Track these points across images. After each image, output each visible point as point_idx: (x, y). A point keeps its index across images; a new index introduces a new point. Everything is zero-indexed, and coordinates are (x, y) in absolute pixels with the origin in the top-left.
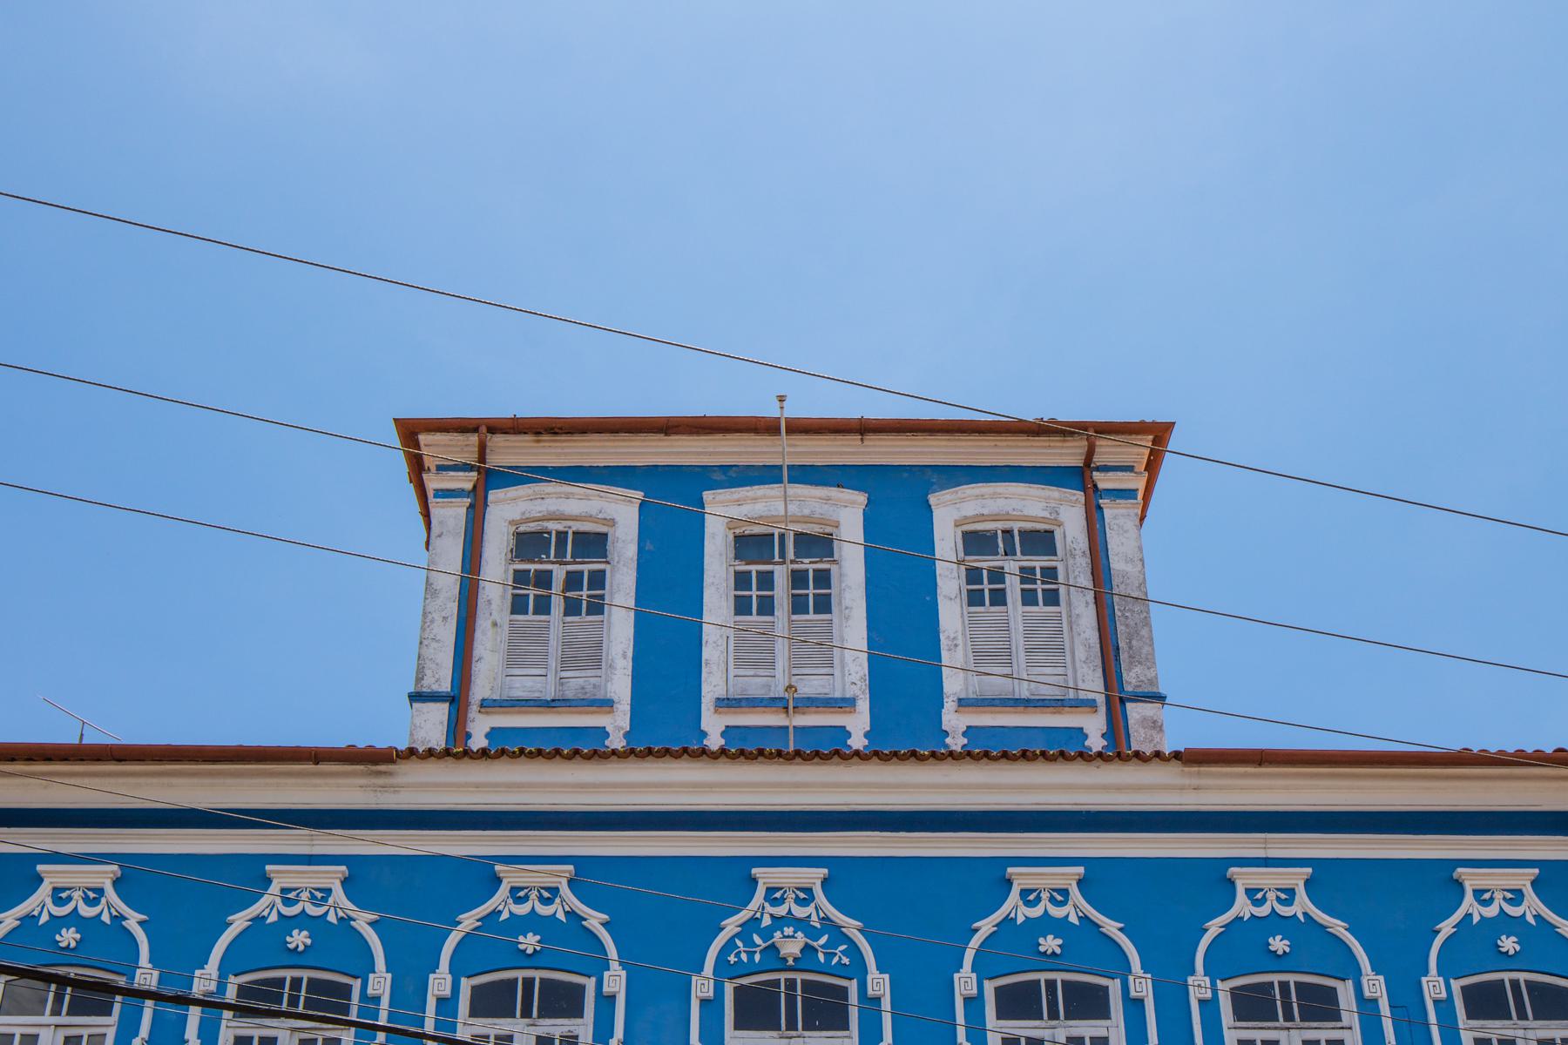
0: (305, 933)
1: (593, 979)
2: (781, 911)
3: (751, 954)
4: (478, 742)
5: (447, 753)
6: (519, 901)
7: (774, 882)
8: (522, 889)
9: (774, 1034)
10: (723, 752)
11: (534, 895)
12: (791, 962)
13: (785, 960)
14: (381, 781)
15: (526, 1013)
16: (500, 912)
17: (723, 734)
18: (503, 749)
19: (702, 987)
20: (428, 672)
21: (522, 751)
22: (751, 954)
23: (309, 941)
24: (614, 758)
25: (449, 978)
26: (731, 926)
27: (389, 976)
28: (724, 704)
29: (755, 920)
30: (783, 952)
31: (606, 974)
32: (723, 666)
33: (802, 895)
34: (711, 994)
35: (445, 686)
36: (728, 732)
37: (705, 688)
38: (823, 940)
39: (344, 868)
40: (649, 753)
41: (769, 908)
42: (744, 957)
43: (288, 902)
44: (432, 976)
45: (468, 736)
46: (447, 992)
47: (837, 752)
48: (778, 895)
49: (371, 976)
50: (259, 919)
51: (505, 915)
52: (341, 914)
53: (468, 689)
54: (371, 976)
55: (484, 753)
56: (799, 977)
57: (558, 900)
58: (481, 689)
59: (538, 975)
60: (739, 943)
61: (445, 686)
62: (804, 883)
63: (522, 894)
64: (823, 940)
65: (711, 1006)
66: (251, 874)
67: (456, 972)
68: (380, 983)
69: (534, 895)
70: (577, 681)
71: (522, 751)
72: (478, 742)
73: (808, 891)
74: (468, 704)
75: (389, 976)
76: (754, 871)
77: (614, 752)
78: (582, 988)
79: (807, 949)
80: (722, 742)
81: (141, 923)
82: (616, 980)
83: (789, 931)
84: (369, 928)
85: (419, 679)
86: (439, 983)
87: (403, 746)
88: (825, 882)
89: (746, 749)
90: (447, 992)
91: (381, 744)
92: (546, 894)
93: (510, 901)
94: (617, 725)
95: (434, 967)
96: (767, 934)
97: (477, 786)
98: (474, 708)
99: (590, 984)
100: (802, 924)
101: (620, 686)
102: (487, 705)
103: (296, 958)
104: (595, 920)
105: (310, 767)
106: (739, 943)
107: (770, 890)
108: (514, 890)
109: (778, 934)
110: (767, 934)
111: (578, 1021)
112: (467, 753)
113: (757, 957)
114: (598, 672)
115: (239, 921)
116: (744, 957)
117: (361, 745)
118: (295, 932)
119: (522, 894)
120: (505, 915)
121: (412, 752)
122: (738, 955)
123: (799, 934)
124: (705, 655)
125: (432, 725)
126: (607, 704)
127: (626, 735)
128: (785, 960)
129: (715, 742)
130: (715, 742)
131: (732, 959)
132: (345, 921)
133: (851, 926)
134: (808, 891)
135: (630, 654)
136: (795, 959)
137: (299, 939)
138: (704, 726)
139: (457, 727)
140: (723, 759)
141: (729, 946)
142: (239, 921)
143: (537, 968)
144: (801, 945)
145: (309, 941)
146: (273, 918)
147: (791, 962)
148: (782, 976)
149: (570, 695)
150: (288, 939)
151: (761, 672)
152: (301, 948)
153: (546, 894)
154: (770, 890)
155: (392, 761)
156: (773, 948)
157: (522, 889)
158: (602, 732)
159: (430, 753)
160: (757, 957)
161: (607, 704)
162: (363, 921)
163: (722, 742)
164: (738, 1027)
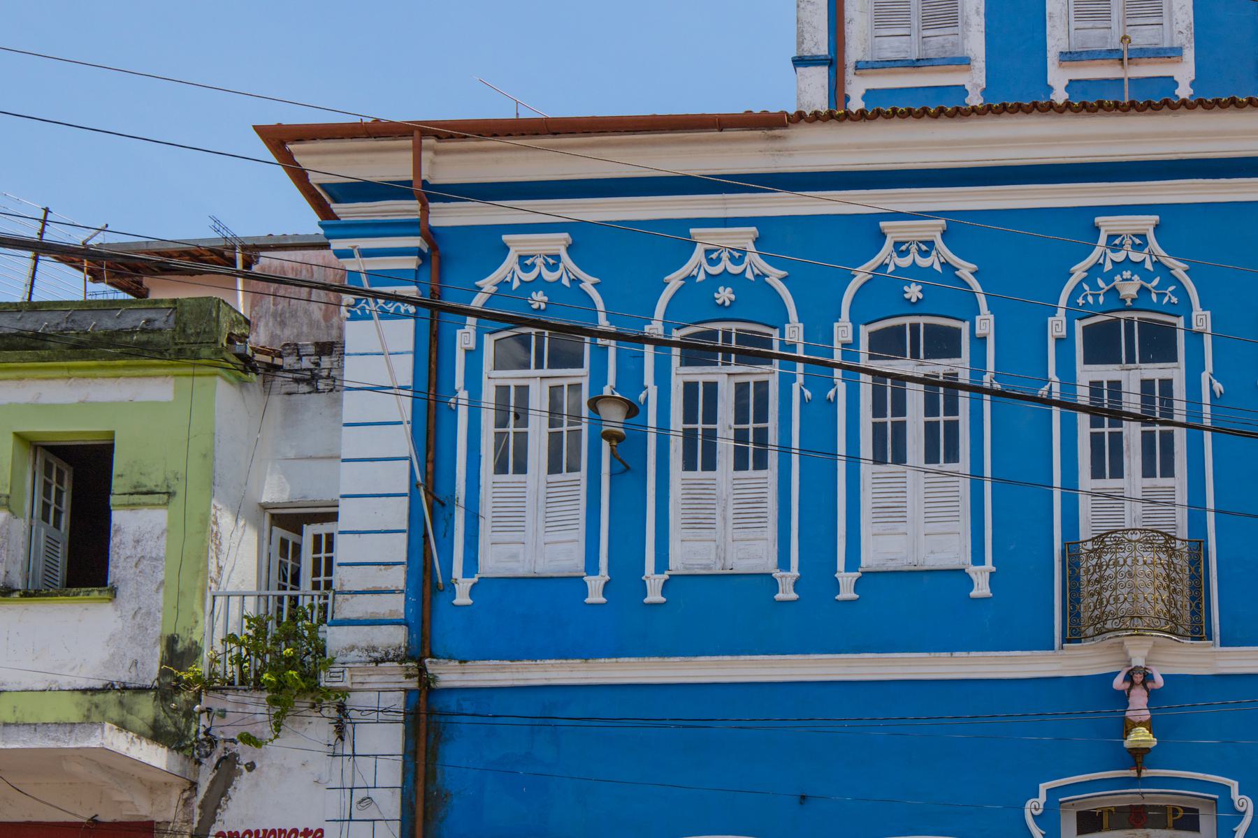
0: (729, 289)
1: (967, 323)
2: (1120, 257)
3: (1096, 296)
4: (856, 105)
5: (830, 116)
6: (902, 254)
7: (1115, 230)
8: (904, 243)
9: (1116, 366)
10: (1068, 106)
11: (914, 248)
12: (1129, 303)
13: (1124, 300)
14: (777, 145)
15: (915, 355)
16: (887, 265)
17: (1067, 88)
18: (880, 110)
19: (1057, 325)
20: (807, 36)
21: (894, 110)
22: (1096, 296)
23: (733, 297)
24: (974, 115)
25: (850, 325)
26: (1079, 271)
27: (801, 325)
28: (1069, 57)
29: (1098, 265)
30: (1123, 293)
31: (978, 318)
32: (1065, 18)
33: (1138, 241)
34: (1064, 333)
35: (823, 50)
36: (1072, 85)
37: (1050, 42)
38: (1156, 282)
39: (754, 229)
40: (1003, 109)
41: (1110, 255)
42: (1090, 299)
43: (712, 262)
44: (836, 325)
45: (847, 98)
46: (849, 339)
47: (1166, 103)
48: (1117, 242)
49: (787, 326)
50: (690, 278)
51: (891, 268)
52: (756, 271)
53: (843, 52)
54: (787, 326)
55: (862, 115)
56: (1136, 316)
57: (934, 253)
58: (854, 52)
59: (922, 321)
60: (1086, 287)
61: (823, 50)
62: (1139, 229)
63: (904, 248)
64: (1156, 282)
65: (1064, 344)
66: (675, 240)
67: (856, 320)
68: (795, 332)
69: (914, 248)
70: (939, 40)
71: (894, 110)
72: (856, 105)
73: (1143, 237)
74: (844, 67)
75: (801, 325)
76: (1097, 220)
77: (974, 109)
78: (959, 331)
79: (1143, 290)
80: (1066, 96)
81: (594, 285)
82: (986, 324)
83: (1127, 274)
84: (780, 283)
85: (800, 43)
86: (842, 331)
87: (792, 111)
88: (1157, 228)
89: (1089, 102)
90: (849, 339)
91: (774, 109)
92: (924, 248)
93: (894, 254)
94: (974, 82)
95: (837, 316)
96: (1109, 278)
97: (859, 147)
98: (850, 70)
99: (965, 327)
100: (1137, 266)
101: (975, 45)
102: (860, 67)
103: (724, 313)
104: (966, 270)
105: (715, 134)
106: (1086, 287)
107: (1111, 237)
108: (897, 244)
109: (1118, 278)
110: (1109, 278)
111: (957, 360)
112: (848, 116)
113: (1101, 299)
114: (955, 30)
115: (674, 281)
116: (1090, 299)
117: (757, 110)
118: (721, 289)
119: (904, 248)
120: (891, 268)
121: (800, 117)
122: (1085, 297)
123: (1136, 277)
124: (1049, 9)
125: (813, 90)
126: (964, 62)
127: (984, 92)
128: (1124, 300)
129: (1060, 96)
130: (1060, 96)
131: (1081, 301)
132: (761, 277)
133: (1179, 268)
134: (1143, 237)
135: (982, 10)
136: (1133, 300)
137: (725, 295)
138: (1050, 81)
139: (837, 90)
140: (1068, 113)
141: (1078, 289)
142: (674, 281)
143: (920, 315)
144: (1138, 287)
145: (733, 297)
146: (701, 277)
147: (1129, 303)
148: (1123, 315)
149: (932, 54)
150: (716, 295)
151: (1099, 24)
152: (727, 303)
153: (924, 248)
154: (1111, 237)
155: (785, 126)
156: (1114, 290)
157: (904, 243)
158: (961, 90)
159: (816, 117)
160: (1101, 299)
161: (964, 62)
162: (775, 276)
163: (1066, 96)
164: (1088, 360)
